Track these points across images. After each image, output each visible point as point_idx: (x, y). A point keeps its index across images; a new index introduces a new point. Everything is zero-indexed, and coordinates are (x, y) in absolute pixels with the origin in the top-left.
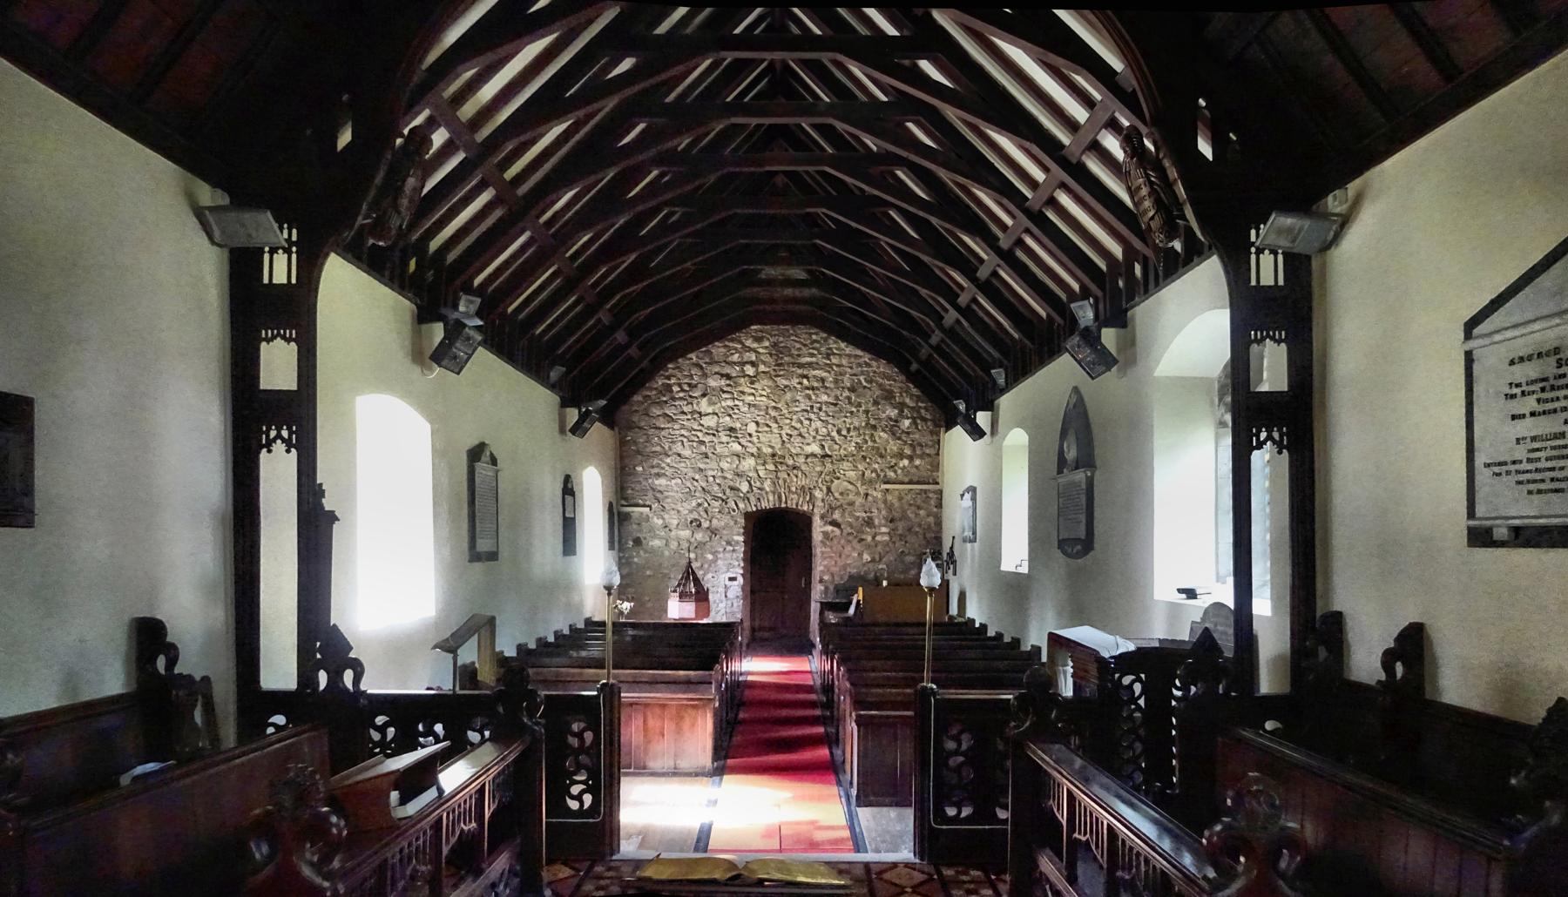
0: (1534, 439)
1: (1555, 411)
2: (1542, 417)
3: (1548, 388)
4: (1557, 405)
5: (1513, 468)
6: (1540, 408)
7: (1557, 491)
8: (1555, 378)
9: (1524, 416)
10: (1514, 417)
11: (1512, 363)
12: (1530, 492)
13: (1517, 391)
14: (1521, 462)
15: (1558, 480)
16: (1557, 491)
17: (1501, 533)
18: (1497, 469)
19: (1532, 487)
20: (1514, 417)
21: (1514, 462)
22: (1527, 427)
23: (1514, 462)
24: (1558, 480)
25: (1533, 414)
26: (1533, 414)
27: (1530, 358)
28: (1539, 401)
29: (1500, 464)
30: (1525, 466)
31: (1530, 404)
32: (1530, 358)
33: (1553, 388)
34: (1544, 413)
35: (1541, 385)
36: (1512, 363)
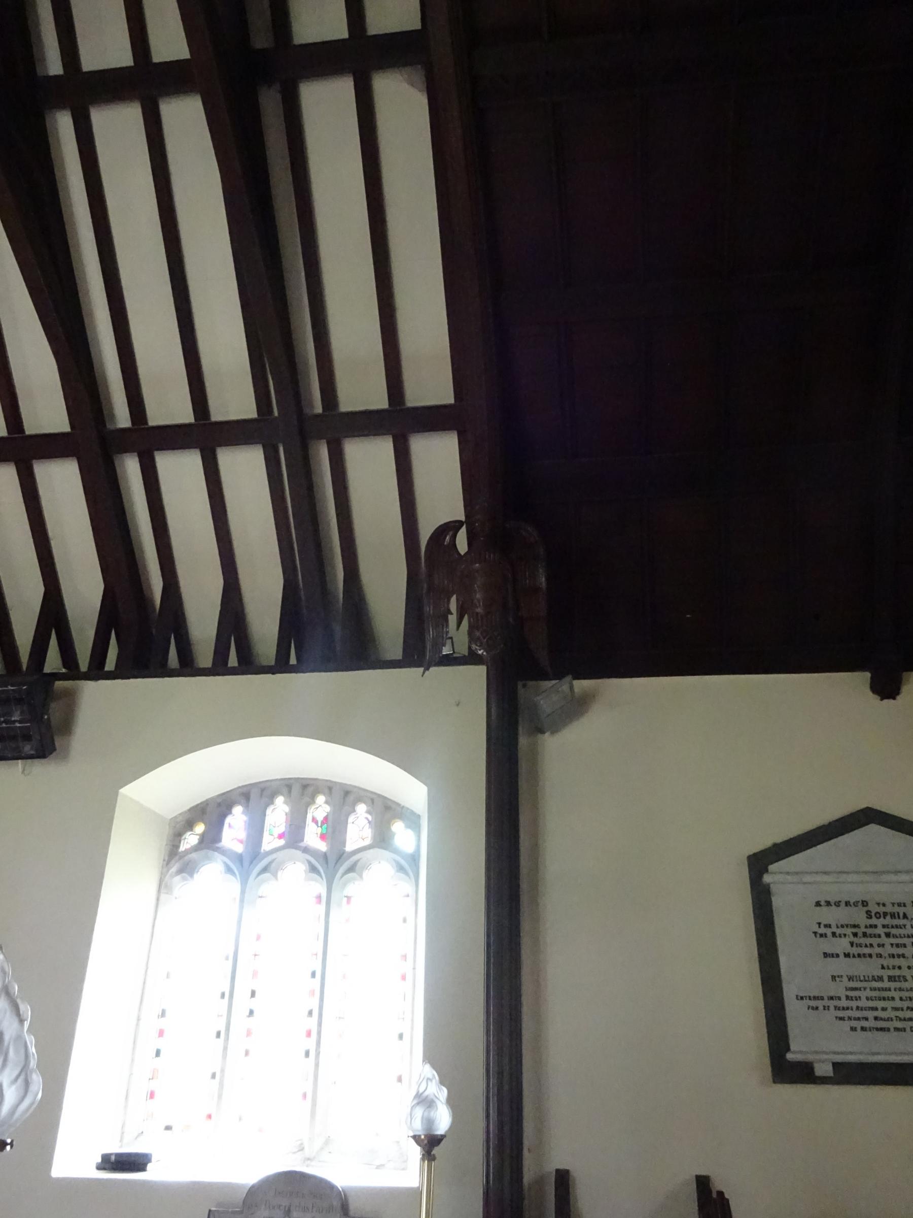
0: (850, 978)
1: (870, 956)
2: (857, 960)
3: (860, 934)
4: (867, 951)
5: (832, 1003)
6: (855, 950)
7: (882, 1029)
8: (866, 927)
9: (838, 956)
10: (826, 955)
11: (818, 904)
12: (853, 1029)
13: (829, 932)
14: (839, 998)
15: (881, 1019)
16: (882, 1029)
17: (823, 1069)
18: (813, 1003)
19: (854, 1023)
20: (826, 955)
21: (831, 998)
22: (841, 966)
23: (831, 998)
24: (881, 1019)
25: (847, 955)
26: (847, 955)
27: (838, 904)
28: (852, 944)
29: (816, 998)
30: (844, 1003)
31: (842, 945)
32: (838, 904)
33: (865, 935)
34: (859, 956)
35: (854, 930)
36: (818, 904)
